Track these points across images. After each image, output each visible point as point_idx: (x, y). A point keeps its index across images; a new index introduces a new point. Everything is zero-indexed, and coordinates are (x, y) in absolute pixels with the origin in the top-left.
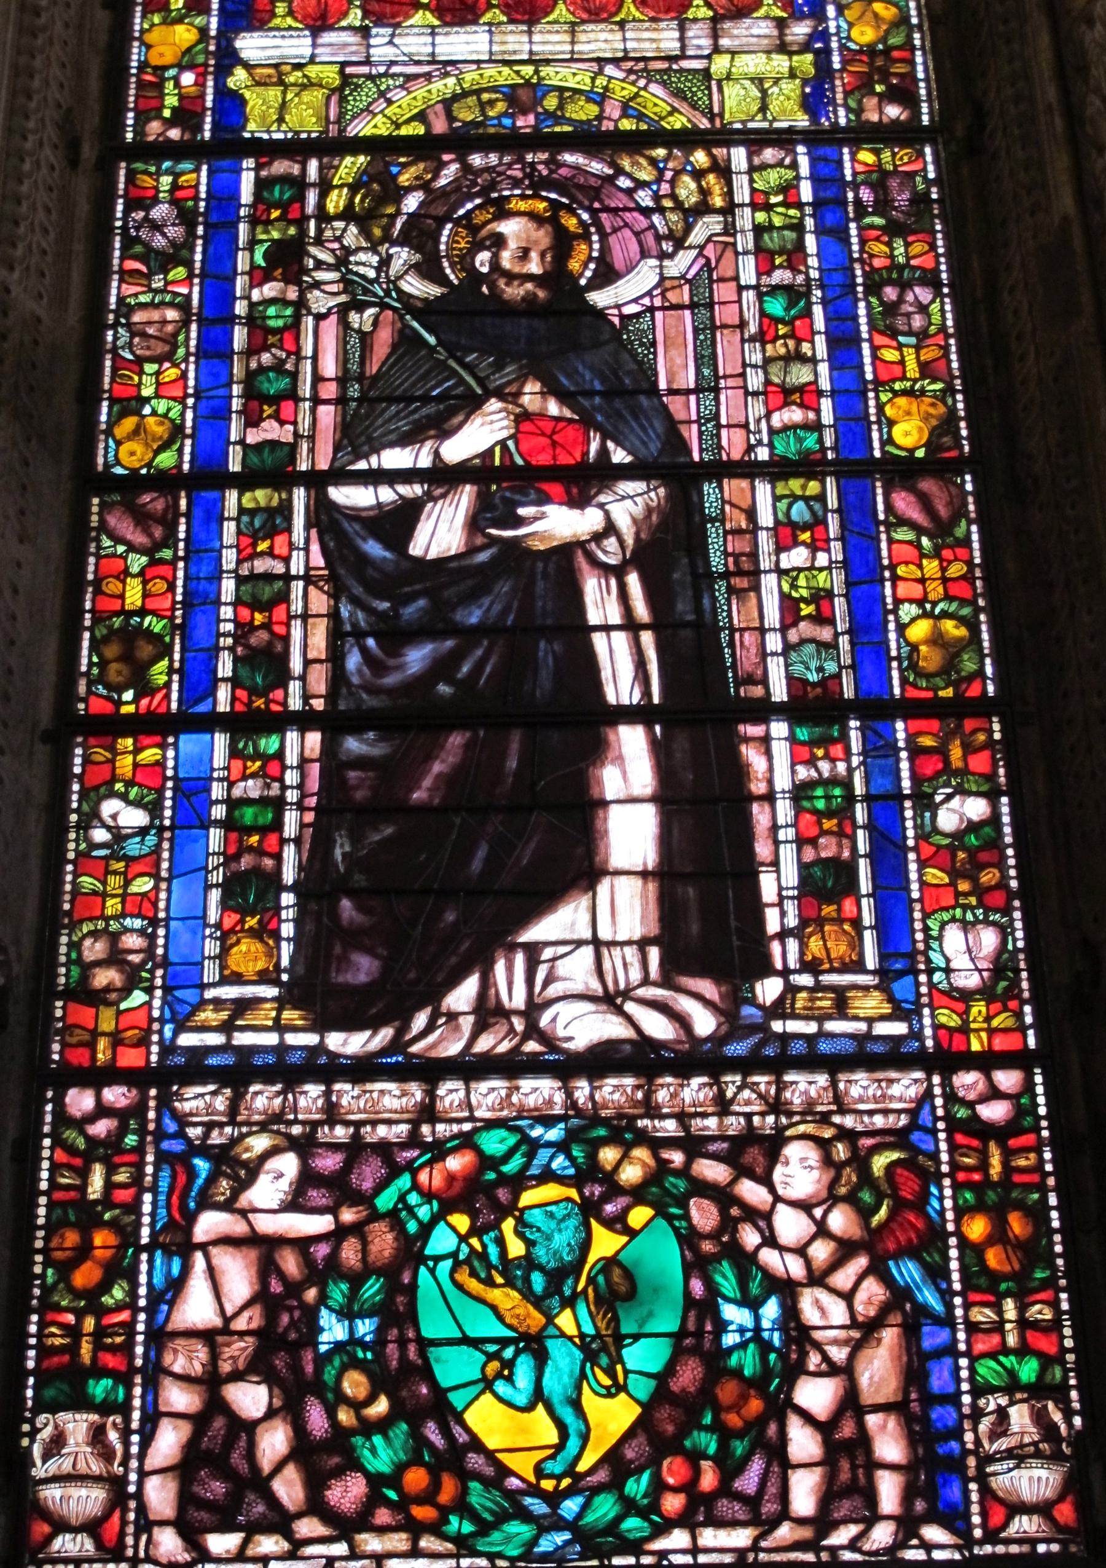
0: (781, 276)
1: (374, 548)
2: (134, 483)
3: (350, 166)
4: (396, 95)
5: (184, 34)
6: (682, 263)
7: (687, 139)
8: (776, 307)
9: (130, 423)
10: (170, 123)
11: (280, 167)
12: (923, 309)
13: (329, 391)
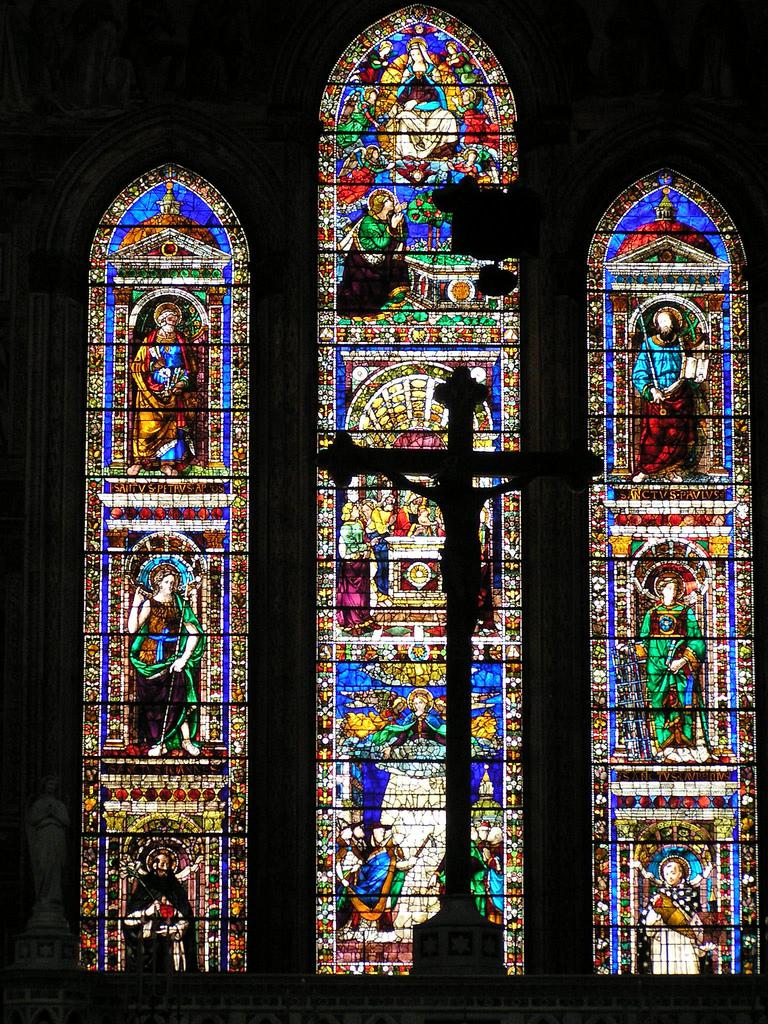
0: (214, 872)
1: (133, 935)
2: (87, 918)
3: (128, 839)
4: (138, 820)
5: (93, 801)
6: (195, 868)
7: (197, 835)
8: (212, 880)
9: (86, 904)
10: (91, 827)
11: (114, 840)
12: (241, 880)
13: (125, 897)
